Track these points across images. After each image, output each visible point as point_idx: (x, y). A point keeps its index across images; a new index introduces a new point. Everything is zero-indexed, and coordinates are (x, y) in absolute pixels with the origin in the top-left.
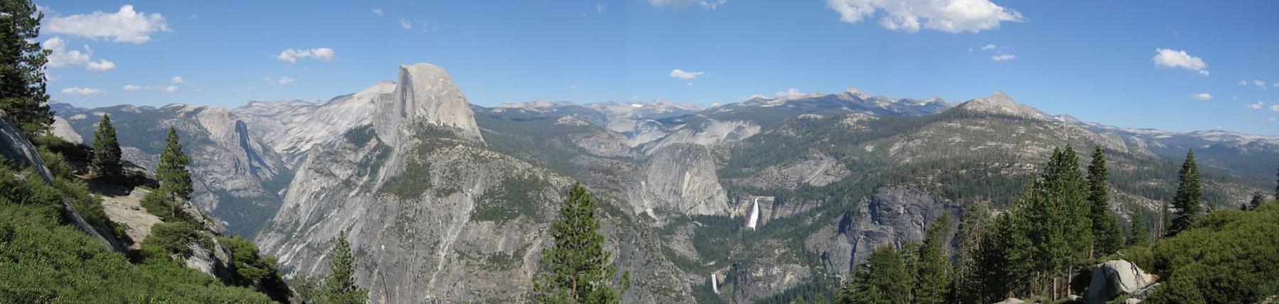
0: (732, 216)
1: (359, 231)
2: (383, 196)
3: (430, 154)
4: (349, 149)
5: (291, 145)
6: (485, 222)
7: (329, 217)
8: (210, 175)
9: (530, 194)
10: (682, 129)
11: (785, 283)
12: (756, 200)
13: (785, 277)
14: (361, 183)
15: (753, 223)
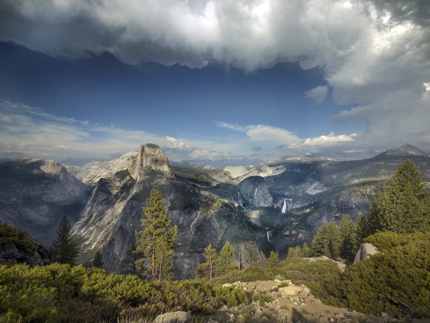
0: (275, 207)
1: (120, 218)
2: (132, 202)
3: (152, 182)
4: (117, 181)
5: (90, 179)
6: (175, 211)
7: (107, 212)
8: (44, 195)
9: (193, 198)
10: (253, 170)
11: (298, 238)
12: (285, 200)
13: (298, 235)
14: (122, 196)
15: (284, 210)
